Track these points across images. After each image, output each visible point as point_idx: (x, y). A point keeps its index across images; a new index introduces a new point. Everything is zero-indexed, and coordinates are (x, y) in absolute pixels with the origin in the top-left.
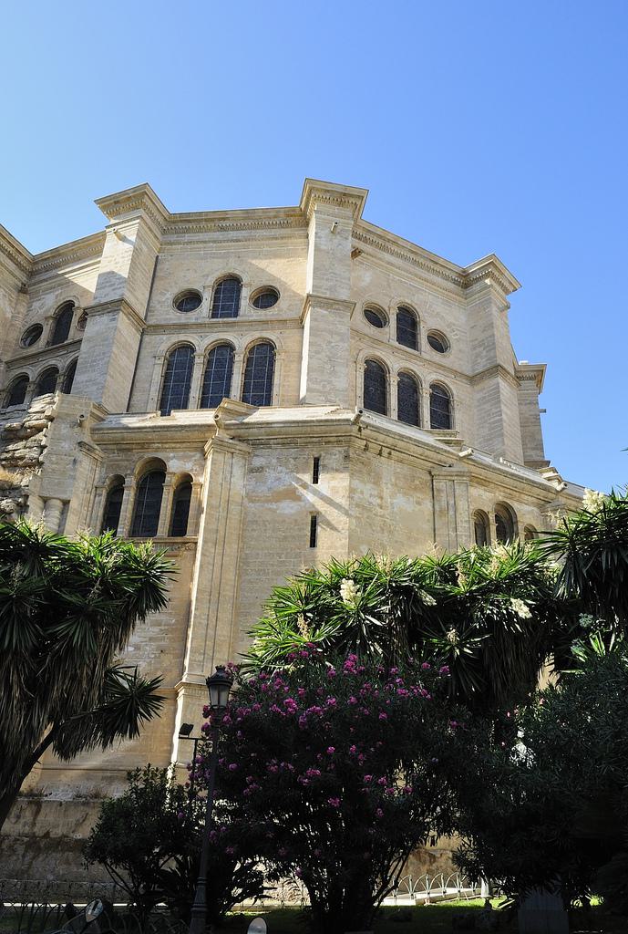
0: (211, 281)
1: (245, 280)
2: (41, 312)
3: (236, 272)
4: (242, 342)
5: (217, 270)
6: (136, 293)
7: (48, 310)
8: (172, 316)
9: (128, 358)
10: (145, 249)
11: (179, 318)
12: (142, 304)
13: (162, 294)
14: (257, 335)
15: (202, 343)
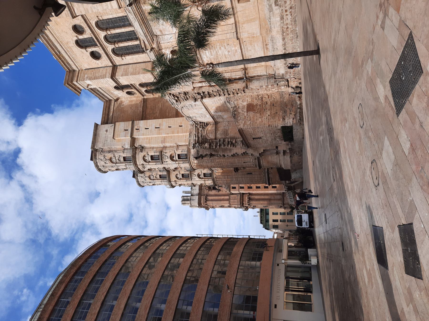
0: (83, 50)
1: (76, 38)
2: (121, 94)
3: (74, 42)
4: (102, 34)
5: (77, 50)
6: (105, 74)
7: (120, 92)
8: (105, 58)
9: (129, 69)
10: (86, 76)
11: (104, 56)
12: (107, 70)
13: (98, 64)
14: (96, 28)
15: (110, 47)
